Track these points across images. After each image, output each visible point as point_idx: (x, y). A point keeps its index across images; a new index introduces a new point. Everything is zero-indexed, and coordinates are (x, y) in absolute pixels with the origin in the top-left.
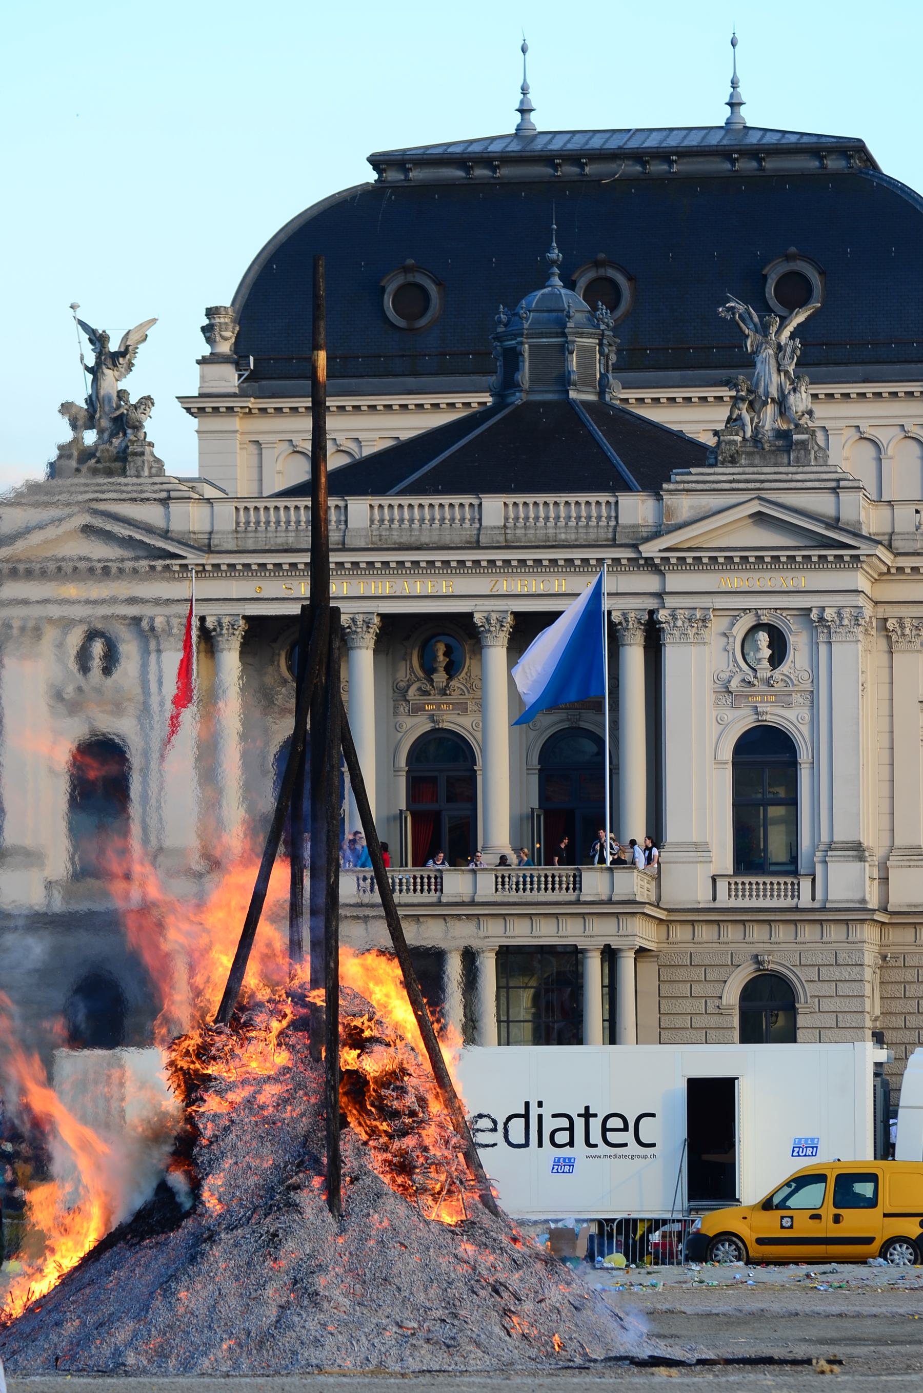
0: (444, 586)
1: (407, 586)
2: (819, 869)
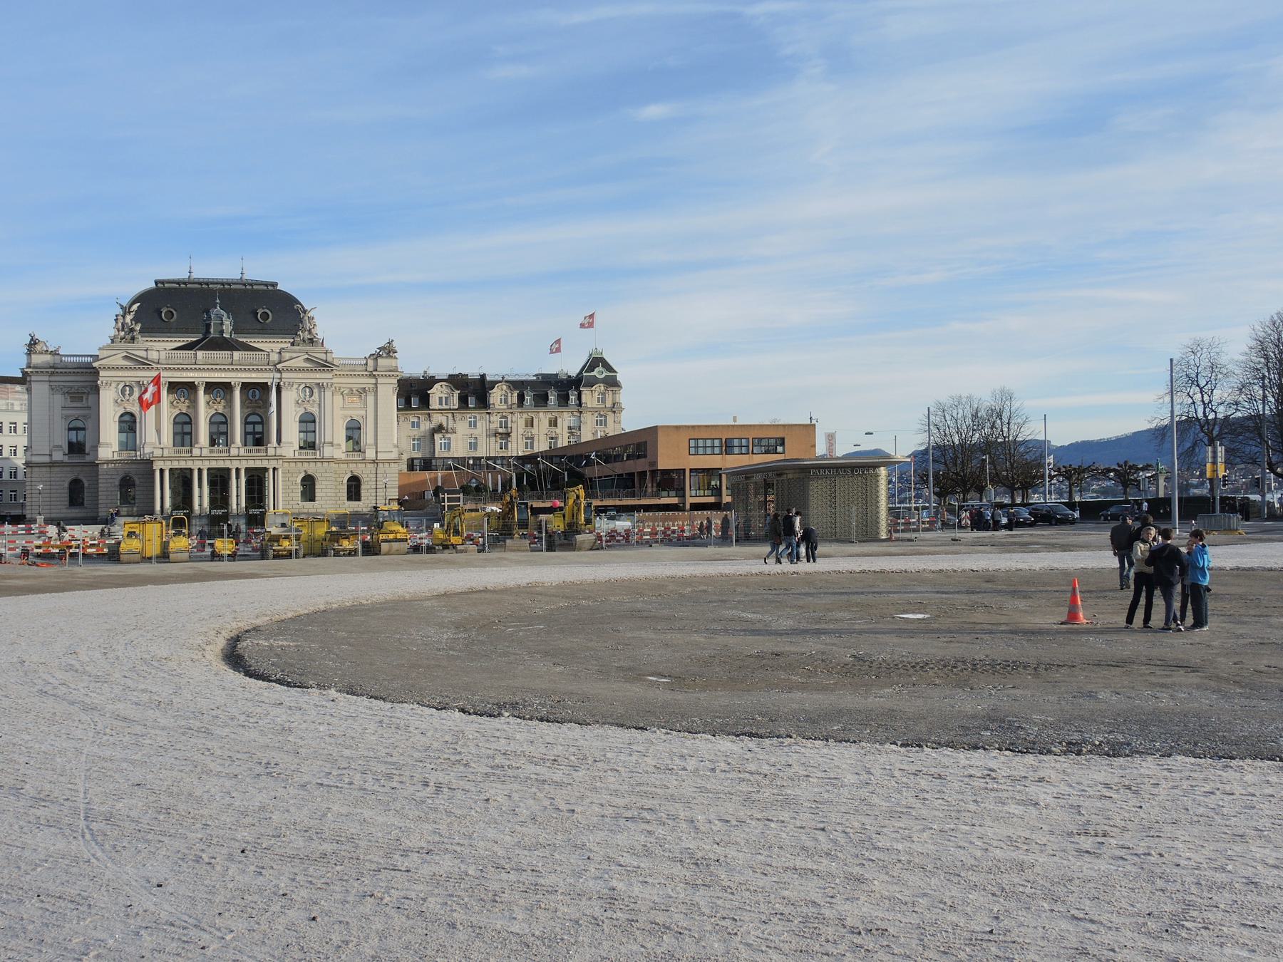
1: (213, 374)
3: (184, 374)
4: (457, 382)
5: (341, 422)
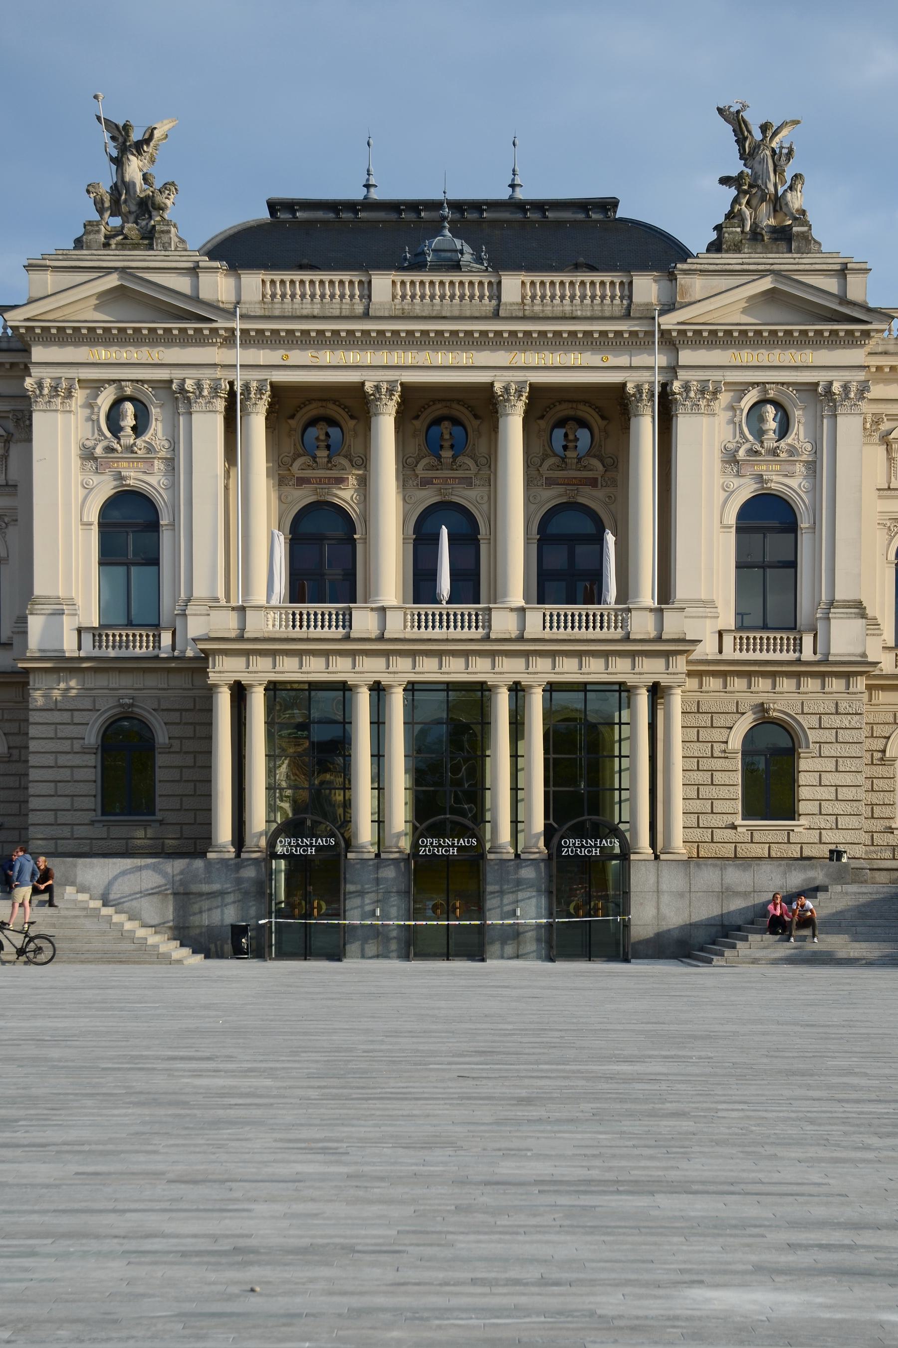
0: (465, 358)
2: (820, 626)
3: (327, 357)
5: (881, 536)
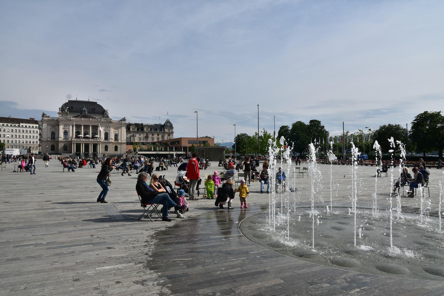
4: (136, 125)
